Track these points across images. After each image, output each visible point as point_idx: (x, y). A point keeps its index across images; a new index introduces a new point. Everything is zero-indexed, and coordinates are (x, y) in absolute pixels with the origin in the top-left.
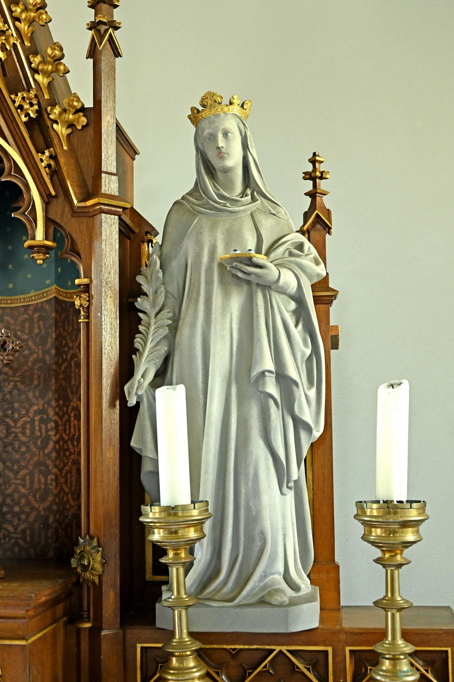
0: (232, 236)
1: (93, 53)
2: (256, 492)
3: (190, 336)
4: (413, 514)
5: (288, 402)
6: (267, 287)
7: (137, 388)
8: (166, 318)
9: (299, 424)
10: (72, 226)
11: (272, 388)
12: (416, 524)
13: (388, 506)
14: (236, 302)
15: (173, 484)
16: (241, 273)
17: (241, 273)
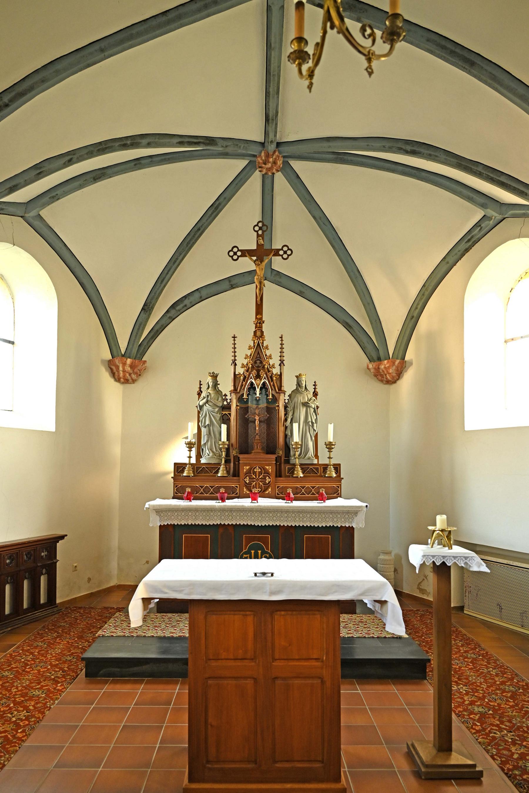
0: (304, 398)
1: (280, 365)
2: (308, 441)
3: (297, 414)
4: (334, 443)
5: (313, 426)
6: (310, 407)
8: (292, 412)
9: (314, 430)
10: (276, 395)
11: (310, 424)
12: (334, 445)
13: (330, 442)
14: (305, 409)
15: (296, 438)
16: (306, 405)
17: (306, 405)
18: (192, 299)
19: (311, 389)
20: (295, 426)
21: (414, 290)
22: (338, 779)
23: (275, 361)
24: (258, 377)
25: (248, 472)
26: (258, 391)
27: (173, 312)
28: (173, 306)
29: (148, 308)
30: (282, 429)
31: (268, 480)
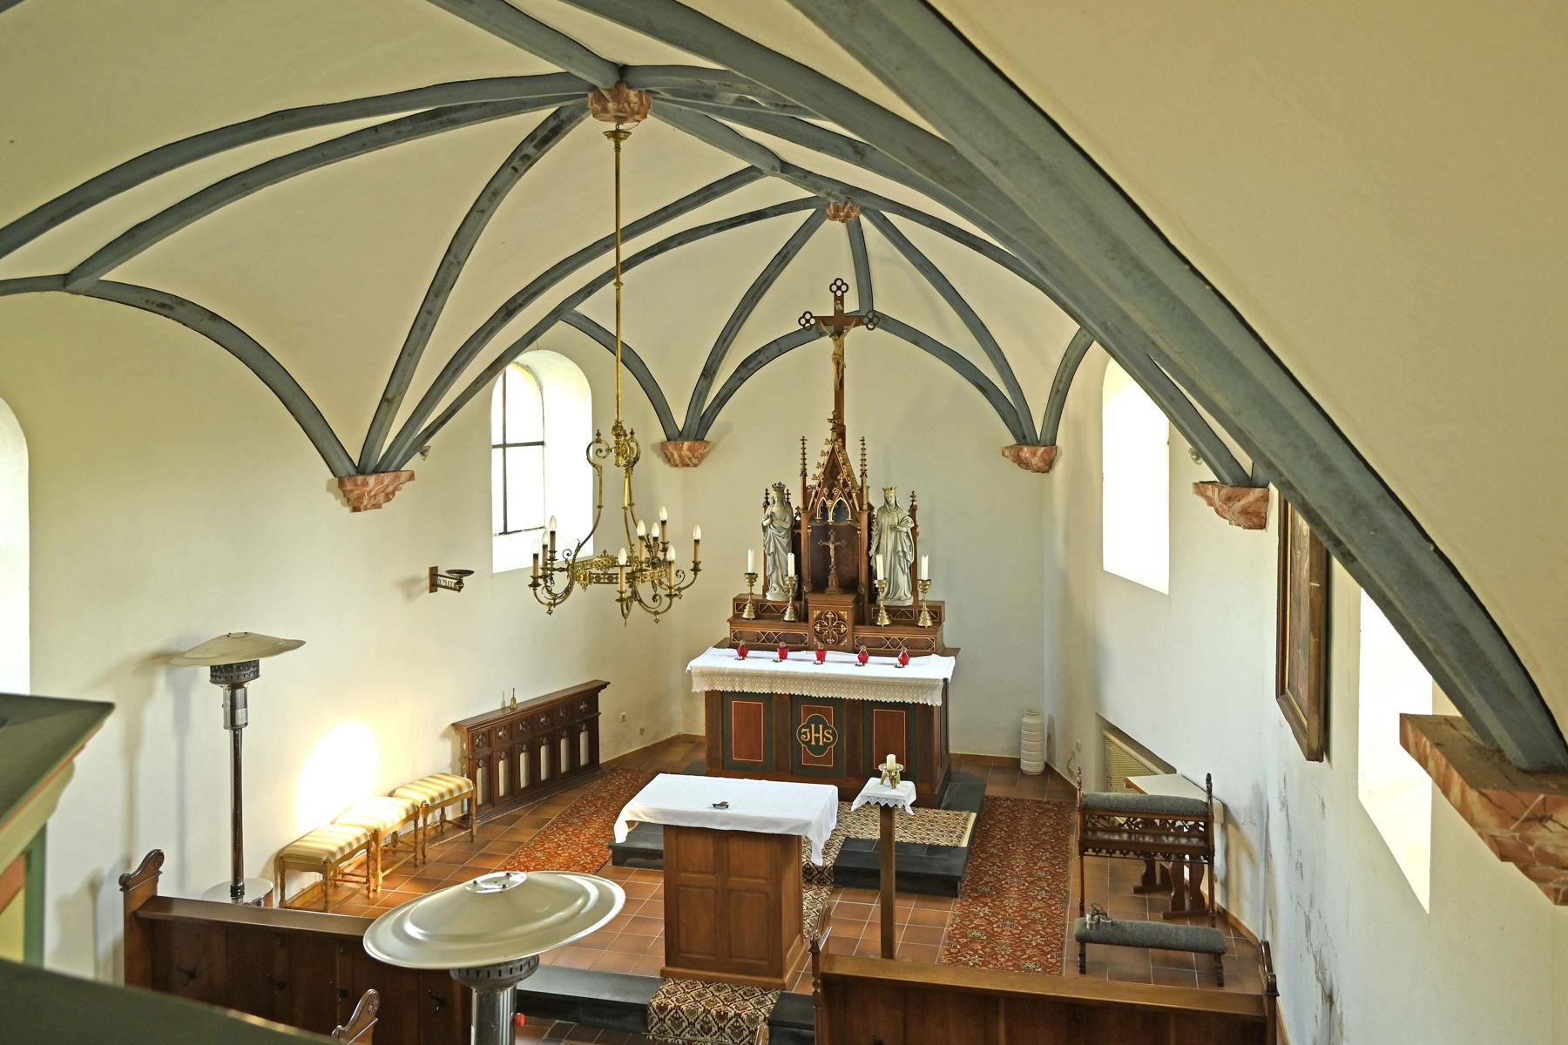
7: (872, 552)
15: (880, 576)
18: (768, 353)
19: (905, 506)
20: (879, 558)
21: (1056, 359)
22: (781, 975)
23: (857, 474)
24: (831, 496)
25: (819, 618)
26: (830, 514)
27: (743, 372)
28: (744, 364)
29: (708, 373)
30: (865, 559)
31: (843, 629)
